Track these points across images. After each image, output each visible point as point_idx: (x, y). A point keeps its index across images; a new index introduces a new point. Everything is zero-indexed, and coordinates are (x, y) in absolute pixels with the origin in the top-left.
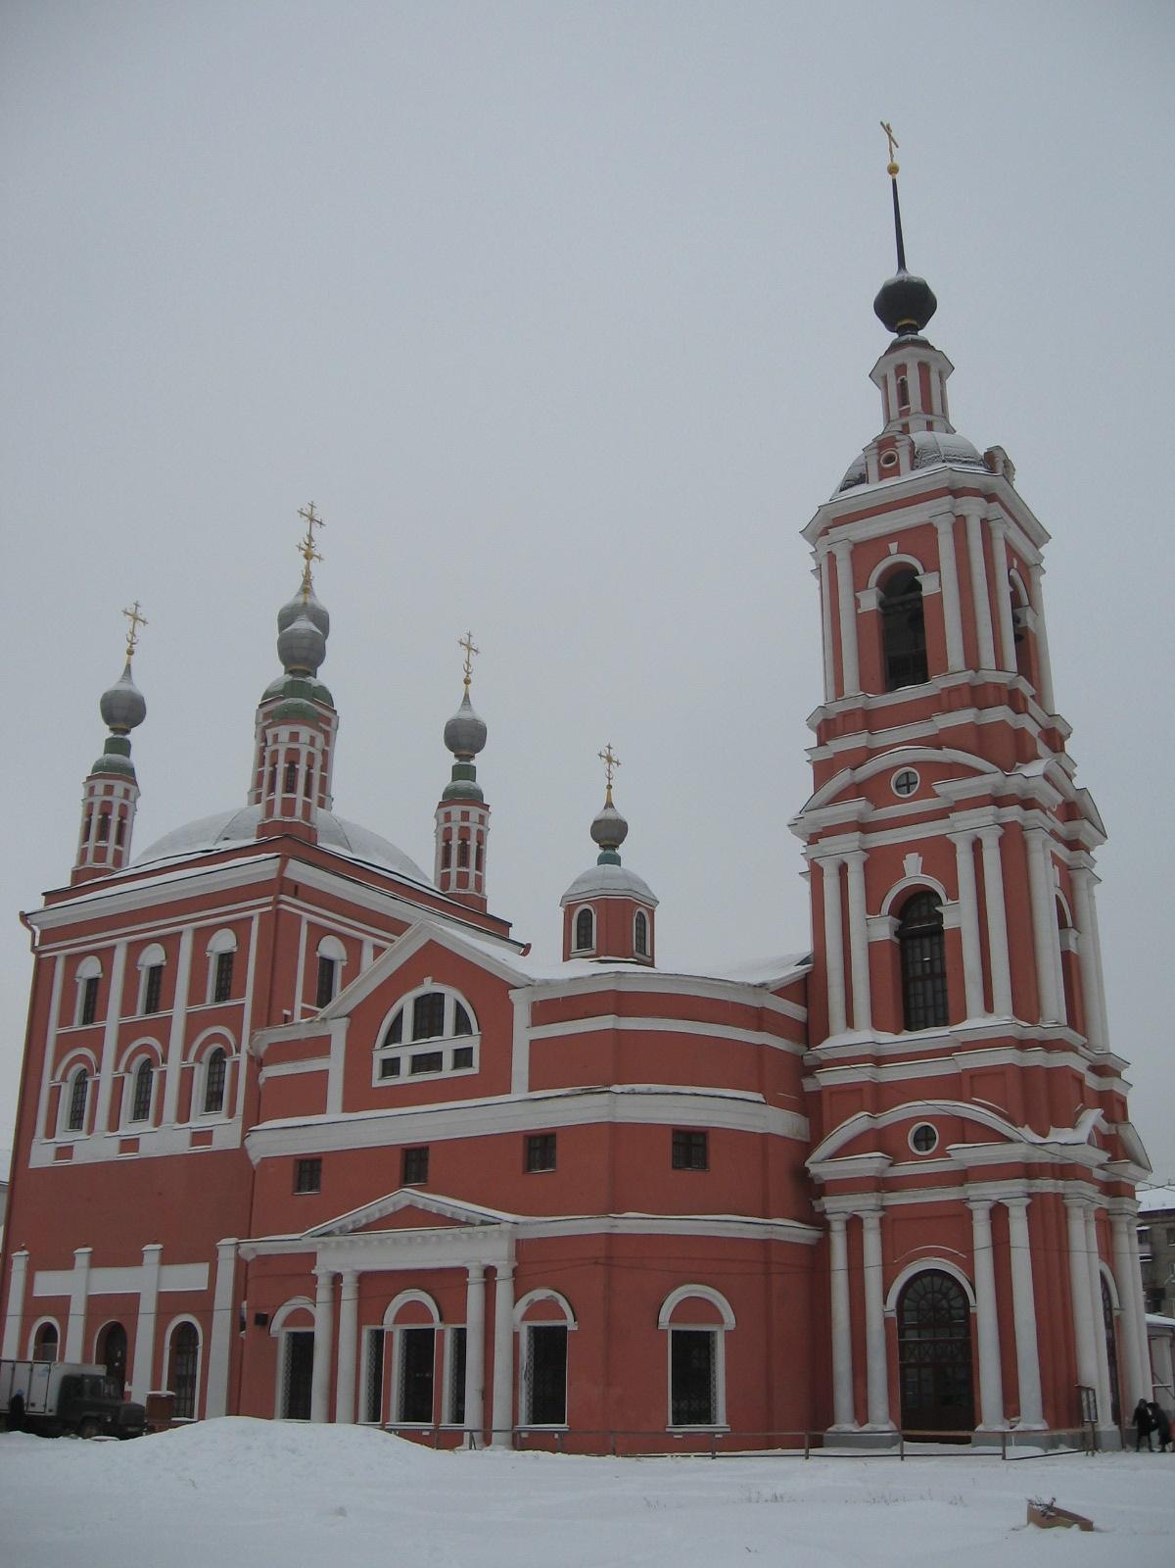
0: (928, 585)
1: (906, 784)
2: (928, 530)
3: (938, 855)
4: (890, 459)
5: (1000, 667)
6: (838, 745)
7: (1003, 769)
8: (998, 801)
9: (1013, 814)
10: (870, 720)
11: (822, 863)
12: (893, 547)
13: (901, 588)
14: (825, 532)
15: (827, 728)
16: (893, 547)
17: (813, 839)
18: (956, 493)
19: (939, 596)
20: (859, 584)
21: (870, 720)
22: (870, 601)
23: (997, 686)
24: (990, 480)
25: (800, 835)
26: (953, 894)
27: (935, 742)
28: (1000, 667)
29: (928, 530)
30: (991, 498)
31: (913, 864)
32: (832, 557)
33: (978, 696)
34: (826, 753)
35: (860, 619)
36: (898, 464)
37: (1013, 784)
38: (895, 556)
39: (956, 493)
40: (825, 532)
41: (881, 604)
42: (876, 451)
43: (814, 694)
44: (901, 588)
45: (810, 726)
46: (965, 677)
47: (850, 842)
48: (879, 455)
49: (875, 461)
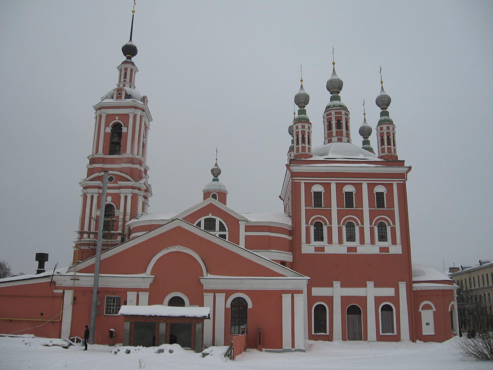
0: (124, 130)
1: (111, 179)
2: (127, 116)
3: (116, 198)
4: (120, 94)
5: (138, 154)
6: (95, 166)
7: (135, 181)
8: (133, 188)
9: (136, 191)
10: (103, 161)
11: (87, 194)
12: (117, 118)
13: (117, 128)
14: (100, 109)
15: (93, 161)
16: (117, 118)
17: (84, 188)
18: (136, 108)
19: (127, 134)
20: (107, 125)
21: (103, 161)
22: (109, 130)
23: (137, 159)
24: (144, 106)
25: (82, 186)
26: (118, 208)
27: (120, 170)
28: (138, 154)
29: (127, 116)
30: (143, 110)
31: (109, 199)
32: (101, 116)
33: (132, 161)
34: (91, 166)
35: (105, 134)
36: (122, 96)
37: (137, 184)
38: (117, 120)
39: (136, 108)
40: (100, 109)
41: (112, 130)
42: (116, 91)
43: (89, 151)
44: (117, 128)
45: (88, 157)
46: (130, 156)
47: (96, 190)
48: (117, 92)
49: (116, 94)
